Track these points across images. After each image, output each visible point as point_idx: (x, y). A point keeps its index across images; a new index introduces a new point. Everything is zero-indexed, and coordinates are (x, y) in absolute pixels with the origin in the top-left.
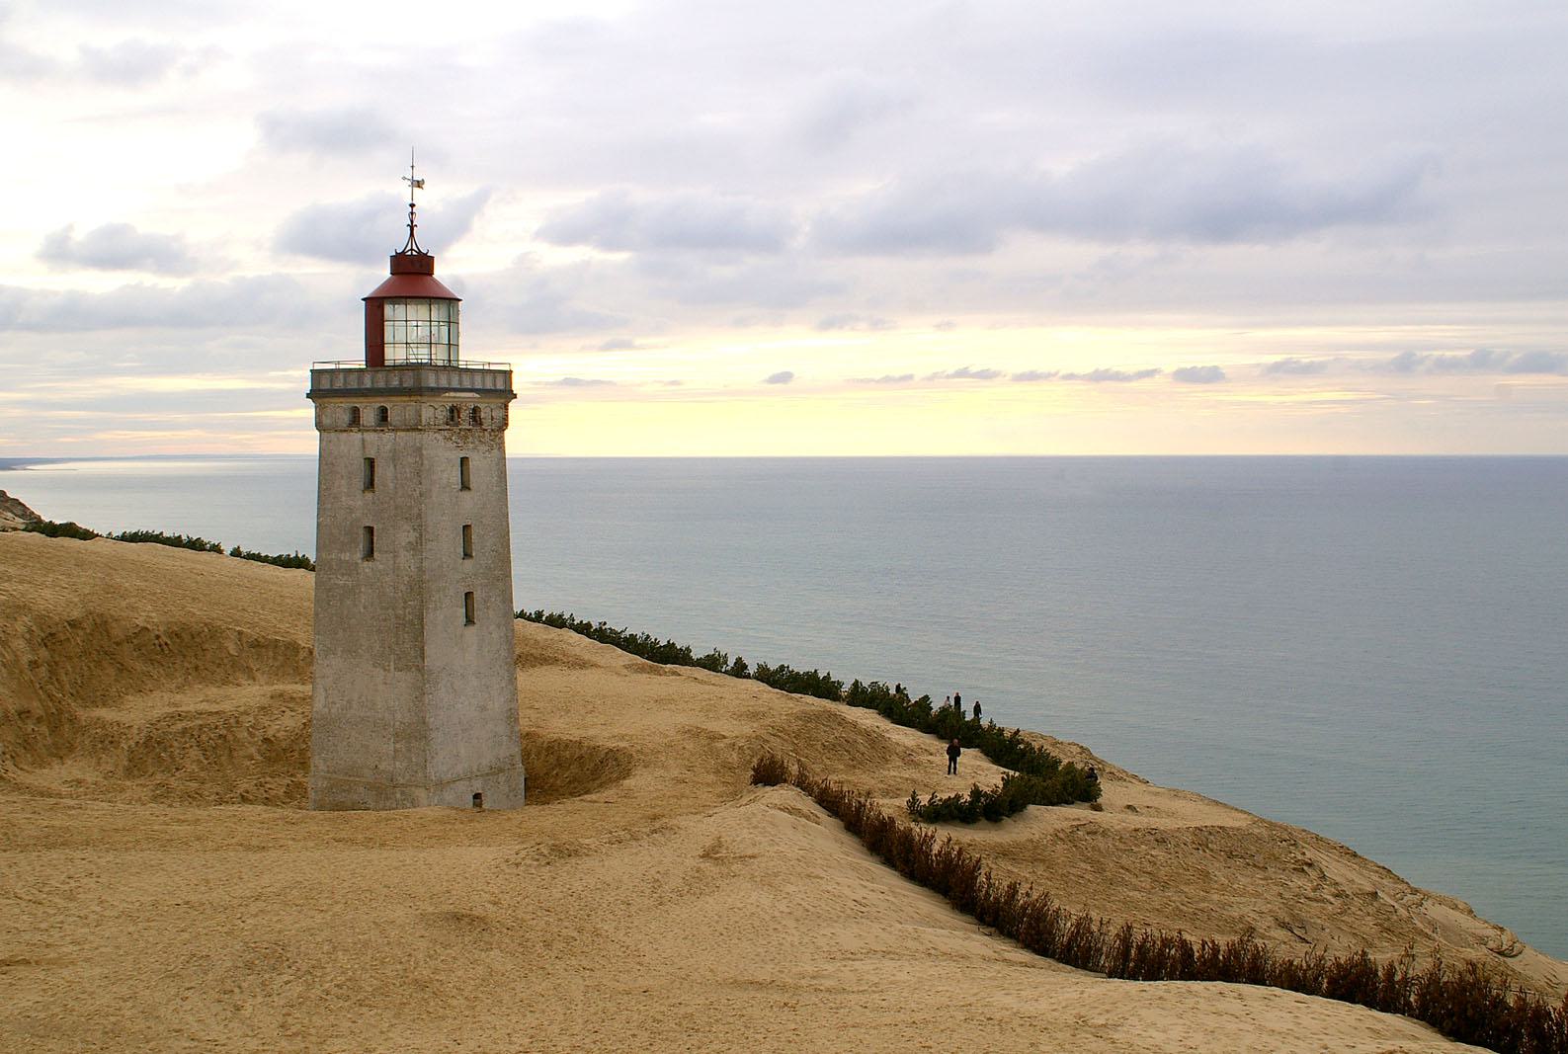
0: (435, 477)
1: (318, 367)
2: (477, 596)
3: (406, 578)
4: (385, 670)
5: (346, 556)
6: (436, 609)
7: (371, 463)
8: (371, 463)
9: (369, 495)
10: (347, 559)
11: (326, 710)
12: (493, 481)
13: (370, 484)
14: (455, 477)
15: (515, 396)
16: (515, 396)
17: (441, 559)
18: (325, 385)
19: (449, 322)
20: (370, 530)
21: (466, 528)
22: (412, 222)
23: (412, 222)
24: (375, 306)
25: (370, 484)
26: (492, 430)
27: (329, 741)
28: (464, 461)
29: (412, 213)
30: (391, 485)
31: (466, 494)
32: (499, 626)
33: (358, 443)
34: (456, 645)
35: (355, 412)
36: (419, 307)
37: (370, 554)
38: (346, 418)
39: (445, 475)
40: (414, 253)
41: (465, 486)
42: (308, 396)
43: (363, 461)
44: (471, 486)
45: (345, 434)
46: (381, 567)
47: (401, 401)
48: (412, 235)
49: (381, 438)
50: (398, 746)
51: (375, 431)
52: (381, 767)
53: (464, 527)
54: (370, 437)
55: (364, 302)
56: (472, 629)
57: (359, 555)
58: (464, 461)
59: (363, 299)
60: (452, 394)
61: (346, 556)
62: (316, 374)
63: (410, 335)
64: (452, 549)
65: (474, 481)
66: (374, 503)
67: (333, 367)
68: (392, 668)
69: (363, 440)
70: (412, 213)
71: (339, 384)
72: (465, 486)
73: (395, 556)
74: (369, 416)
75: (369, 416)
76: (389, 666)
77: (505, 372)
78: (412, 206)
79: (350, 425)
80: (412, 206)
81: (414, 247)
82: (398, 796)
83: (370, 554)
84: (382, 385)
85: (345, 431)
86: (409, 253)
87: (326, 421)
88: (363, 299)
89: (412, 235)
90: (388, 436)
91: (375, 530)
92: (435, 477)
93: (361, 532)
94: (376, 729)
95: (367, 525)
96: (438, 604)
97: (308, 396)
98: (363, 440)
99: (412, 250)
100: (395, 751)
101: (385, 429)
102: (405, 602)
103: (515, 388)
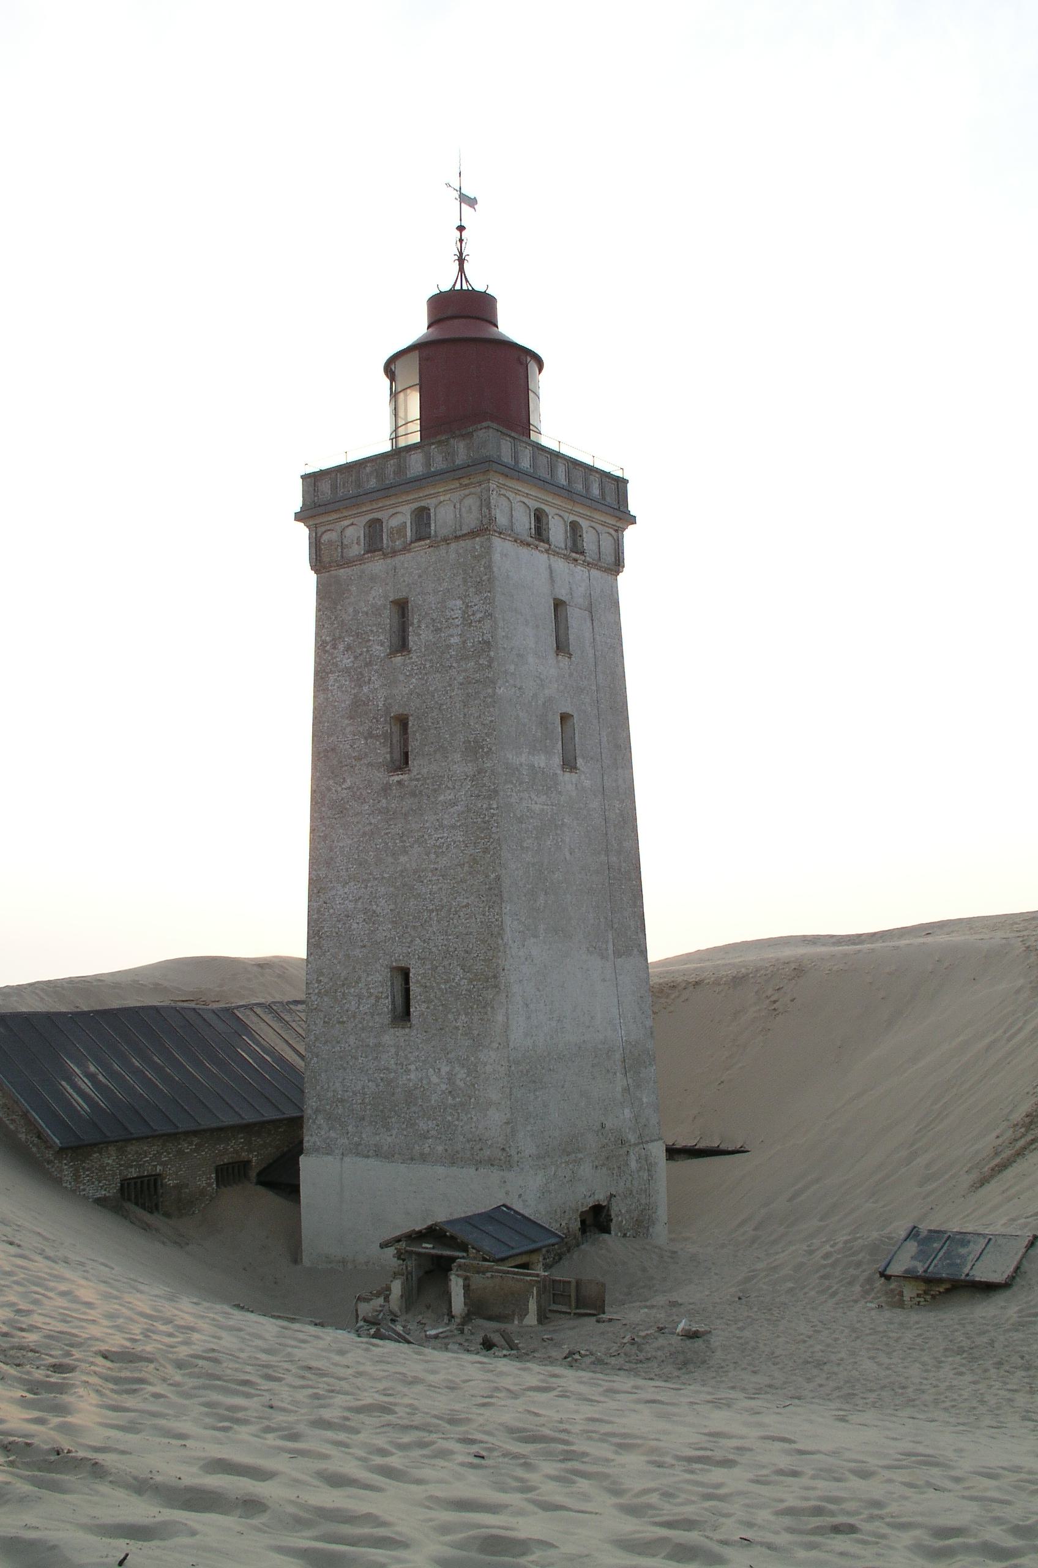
5: (540, 761)
7: (559, 605)
9: (564, 661)
10: (542, 765)
22: (461, 253)
37: (569, 764)
45: (524, 551)
48: (461, 270)
51: (566, 557)
52: (608, 1125)
57: (557, 761)
61: (540, 761)
66: (571, 675)
68: (610, 952)
70: (461, 240)
75: (557, 532)
76: (607, 949)
78: (461, 228)
80: (461, 228)
82: (633, 1165)
83: (569, 764)
85: (528, 545)
89: (461, 270)
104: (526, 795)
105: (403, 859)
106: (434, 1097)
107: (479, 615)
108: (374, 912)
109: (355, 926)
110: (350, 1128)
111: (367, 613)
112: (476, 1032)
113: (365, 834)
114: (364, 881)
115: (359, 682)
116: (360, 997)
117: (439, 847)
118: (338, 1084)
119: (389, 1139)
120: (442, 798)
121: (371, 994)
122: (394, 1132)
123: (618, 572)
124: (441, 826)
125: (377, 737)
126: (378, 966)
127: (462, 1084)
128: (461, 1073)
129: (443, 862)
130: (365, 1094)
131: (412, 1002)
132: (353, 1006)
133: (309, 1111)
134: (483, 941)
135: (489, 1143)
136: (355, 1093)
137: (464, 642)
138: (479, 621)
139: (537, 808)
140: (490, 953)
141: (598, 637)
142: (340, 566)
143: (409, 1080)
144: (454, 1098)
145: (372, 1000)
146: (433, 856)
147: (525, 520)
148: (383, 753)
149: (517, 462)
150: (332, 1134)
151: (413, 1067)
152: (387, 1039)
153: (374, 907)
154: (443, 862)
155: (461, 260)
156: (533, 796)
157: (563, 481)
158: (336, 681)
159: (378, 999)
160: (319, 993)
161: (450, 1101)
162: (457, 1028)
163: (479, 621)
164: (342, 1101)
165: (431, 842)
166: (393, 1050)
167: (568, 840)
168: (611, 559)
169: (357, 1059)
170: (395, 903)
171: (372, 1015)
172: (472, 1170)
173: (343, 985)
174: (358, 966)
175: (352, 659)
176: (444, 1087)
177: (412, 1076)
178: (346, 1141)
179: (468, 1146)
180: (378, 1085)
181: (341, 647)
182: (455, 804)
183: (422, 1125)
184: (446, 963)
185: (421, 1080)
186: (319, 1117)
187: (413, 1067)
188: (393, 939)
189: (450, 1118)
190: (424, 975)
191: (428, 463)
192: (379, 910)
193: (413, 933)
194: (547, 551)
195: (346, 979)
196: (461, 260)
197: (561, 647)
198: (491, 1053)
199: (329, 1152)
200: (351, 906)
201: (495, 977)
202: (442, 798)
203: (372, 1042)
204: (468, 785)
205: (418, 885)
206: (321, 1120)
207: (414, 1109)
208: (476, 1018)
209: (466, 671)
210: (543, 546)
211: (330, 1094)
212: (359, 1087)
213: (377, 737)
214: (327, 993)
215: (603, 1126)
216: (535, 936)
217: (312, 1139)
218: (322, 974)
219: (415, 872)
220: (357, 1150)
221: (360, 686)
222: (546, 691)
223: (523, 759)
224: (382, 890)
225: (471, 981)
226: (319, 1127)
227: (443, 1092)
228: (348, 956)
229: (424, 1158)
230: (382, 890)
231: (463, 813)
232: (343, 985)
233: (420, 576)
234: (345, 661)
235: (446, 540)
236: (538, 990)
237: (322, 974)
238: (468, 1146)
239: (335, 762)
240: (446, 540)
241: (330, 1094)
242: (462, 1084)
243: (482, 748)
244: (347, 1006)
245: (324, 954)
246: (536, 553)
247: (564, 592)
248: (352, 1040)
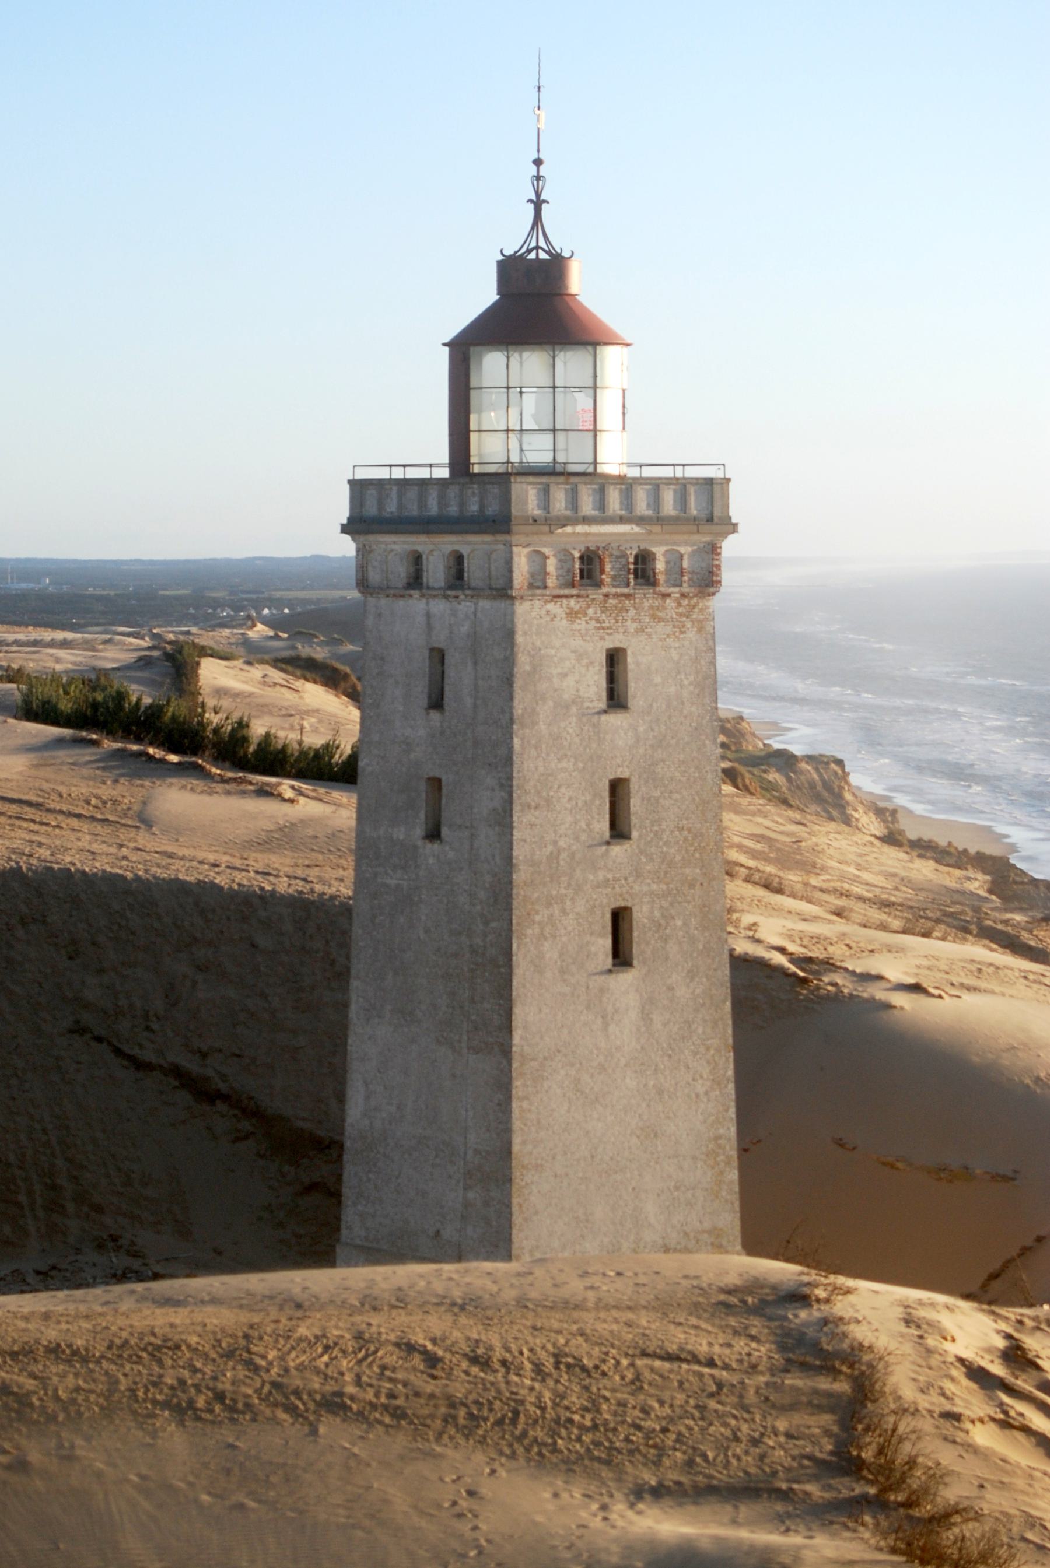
0: (543, 686)
1: (362, 474)
2: (641, 916)
3: (488, 878)
6: (542, 936)
7: (438, 656)
8: (438, 656)
9: (435, 715)
10: (401, 837)
11: (367, 1122)
12: (685, 694)
13: (437, 702)
14: (593, 683)
15: (734, 528)
16: (734, 528)
17: (555, 843)
18: (371, 509)
19: (554, 387)
20: (436, 784)
21: (617, 789)
22: (538, 194)
23: (538, 194)
24: (464, 351)
25: (437, 702)
26: (683, 595)
27: (369, 1180)
28: (614, 659)
29: (538, 178)
30: (469, 701)
31: (616, 719)
32: (692, 975)
33: (421, 619)
34: (588, 1008)
35: (417, 559)
36: (526, 354)
37: (434, 834)
38: (401, 571)
39: (570, 681)
40: (543, 256)
41: (616, 698)
42: (345, 529)
43: (427, 653)
44: (630, 704)
45: (401, 603)
46: (451, 855)
47: (483, 543)
49: (454, 613)
50: (471, 1195)
53: (439, 781)
54: (439, 607)
55: (447, 348)
56: (626, 978)
57: (419, 831)
58: (614, 659)
59: (444, 345)
60: (580, 529)
61: (400, 833)
62: (359, 488)
63: (520, 409)
64: (583, 825)
65: (635, 689)
67: (383, 474)
68: (464, 1045)
69: (428, 615)
70: (538, 178)
71: (391, 508)
72: (616, 698)
73: (472, 835)
74: (436, 572)
75: (436, 572)
76: (460, 1042)
77: (710, 482)
78: (538, 162)
79: (410, 586)
80: (538, 162)
81: (542, 243)
83: (434, 834)
84: (453, 510)
85: (402, 596)
86: (532, 256)
87: (374, 577)
88: (444, 345)
90: (465, 606)
91: (444, 783)
92: (543, 686)
93: (423, 786)
94: (438, 1161)
95: (431, 774)
96: (548, 930)
97: (345, 529)
98: (428, 615)
99: (537, 248)
100: (467, 1205)
101: (459, 593)
102: (486, 923)
103: (735, 513)
139: (393, 882)
141: (480, 683)
155: (538, 204)
156: (390, 871)
167: (423, 918)
194: (423, 596)
196: (538, 204)
210: (416, 593)
215: (438, 1233)
216: (379, 1017)
222: (412, 756)
223: (381, 832)
236: (380, 1072)
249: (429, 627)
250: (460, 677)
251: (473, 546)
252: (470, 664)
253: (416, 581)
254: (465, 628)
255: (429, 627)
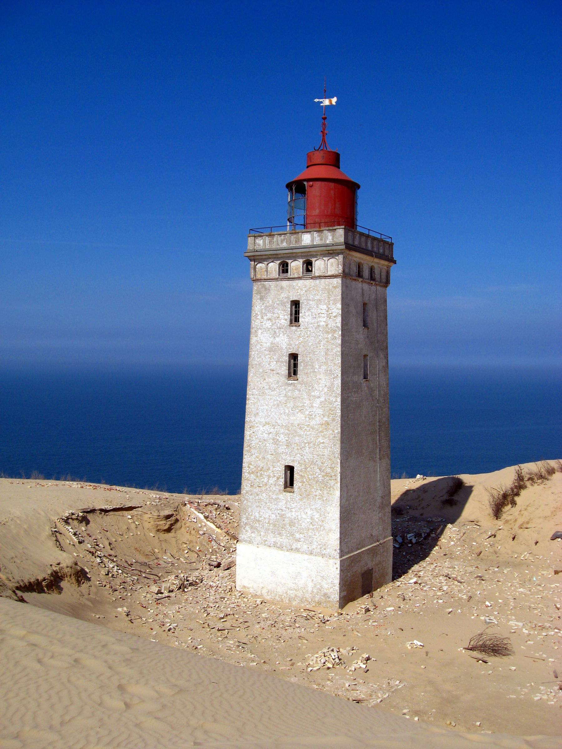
4: (374, 461)
5: (356, 378)
30: (375, 325)
33: (360, 291)
45: (354, 282)
48: (324, 140)
52: (374, 534)
57: (362, 377)
61: (356, 378)
69: (363, 289)
70: (324, 124)
98: (363, 289)
104: (350, 395)
105: (292, 418)
106: (303, 524)
107: (334, 314)
108: (278, 440)
109: (268, 445)
110: (262, 533)
111: (278, 304)
112: (325, 498)
113: (274, 405)
114: (273, 425)
115: (274, 335)
116: (269, 477)
117: (311, 415)
118: (257, 514)
119: (281, 540)
120: (313, 394)
121: (275, 476)
122: (284, 537)
123: (387, 287)
124: (312, 406)
125: (282, 362)
126: (279, 464)
127: (317, 520)
128: (317, 516)
129: (313, 423)
130: (270, 519)
131: (295, 482)
132: (266, 480)
133: (242, 524)
134: (330, 459)
135: (329, 546)
136: (265, 518)
137: (327, 325)
138: (335, 317)
140: (333, 465)
142: (266, 280)
143: (292, 515)
144: (313, 525)
145: (275, 479)
146: (307, 419)
147: (355, 269)
148: (284, 370)
149: (354, 242)
150: (253, 535)
151: (293, 510)
152: (281, 496)
153: (278, 438)
154: (313, 423)
157: (370, 248)
158: (262, 333)
159: (278, 478)
160: (249, 472)
161: (311, 526)
162: (316, 495)
163: (335, 317)
164: (259, 521)
165: (307, 413)
166: (284, 502)
168: (384, 280)
169: (266, 503)
170: (288, 438)
171: (275, 485)
172: (321, 558)
173: (261, 470)
174: (269, 463)
175: (271, 324)
176: (308, 520)
177: (293, 514)
178: (260, 539)
179: (319, 547)
180: (276, 516)
181: (265, 318)
182: (319, 397)
183: (297, 536)
184: (312, 466)
185: (298, 516)
186: (247, 527)
187: (293, 510)
188: (286, 453)
189: (310, 534)
190: (301, 471)
191: (313, 240)
192: (280, 439)
193: (296, 451)
195: (263, 468)
197: (365, 325)
198: (332, 508)
199: (250, 542)
200: (266, 436)
201: (335, 476)
202: (313, 394)
203: (274, 497)
204: (326, 390)
205: (299, 431)
206: (247, 528)
207: (295, 528)
208: (325, 492)
209: (327, 338)
210: (361, 280)
211: (252, 517)
212: (267, 516)
213: (282, 362)
214: (253, 473)
215: (372, 535)
217: (243, 536)
218: (251, 464)
219: (298, 425)
220: (264, 543)
221: (275, 338)
224: (282, 431)
225: (323, 476)
226: (247, 531)
227: (308, 522)
228: (264, 458)
229: (297, 550)
230: (282, 431)
231: (323, 402)
232: (261, 470)
233: (306, 291)
234: (267, 325)
235: (320, 277)
237: (251, 464)
238: (319, 547)
239: (261, 370)
240: (320, 277)
241: (252, 517)
242: (317, 520)
243: (334, 374)
244: (263, 480)
245: (252, 455)
246: (357, 283)
247: (367, 299)
248: (264, 495)
249: (363, 294)
250: (372, 315)
251: (379, 264)
252: (375, 310)
253: (360, 275)
254: (373, 297)
255: (363, 294)
